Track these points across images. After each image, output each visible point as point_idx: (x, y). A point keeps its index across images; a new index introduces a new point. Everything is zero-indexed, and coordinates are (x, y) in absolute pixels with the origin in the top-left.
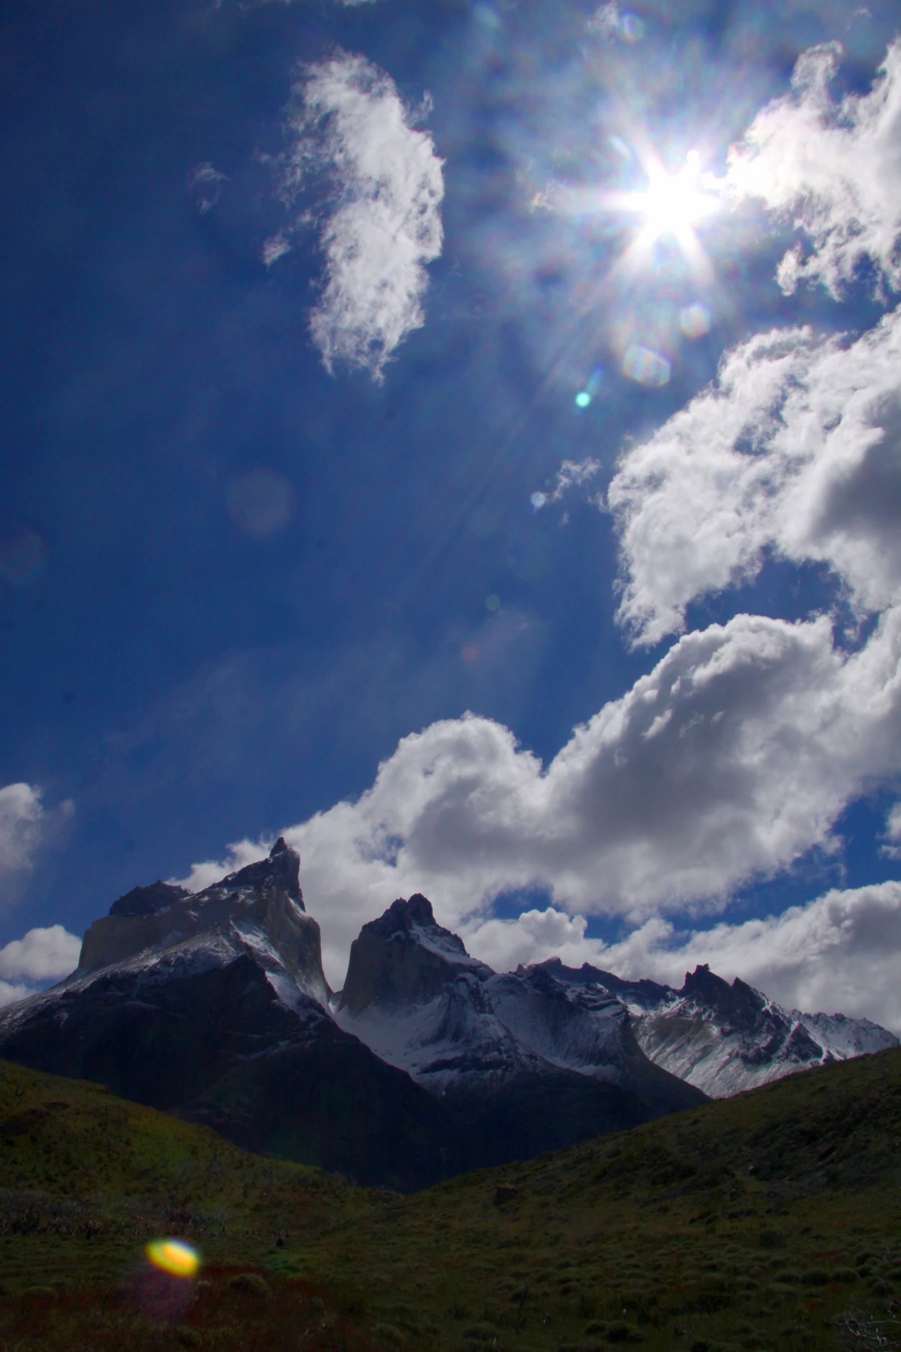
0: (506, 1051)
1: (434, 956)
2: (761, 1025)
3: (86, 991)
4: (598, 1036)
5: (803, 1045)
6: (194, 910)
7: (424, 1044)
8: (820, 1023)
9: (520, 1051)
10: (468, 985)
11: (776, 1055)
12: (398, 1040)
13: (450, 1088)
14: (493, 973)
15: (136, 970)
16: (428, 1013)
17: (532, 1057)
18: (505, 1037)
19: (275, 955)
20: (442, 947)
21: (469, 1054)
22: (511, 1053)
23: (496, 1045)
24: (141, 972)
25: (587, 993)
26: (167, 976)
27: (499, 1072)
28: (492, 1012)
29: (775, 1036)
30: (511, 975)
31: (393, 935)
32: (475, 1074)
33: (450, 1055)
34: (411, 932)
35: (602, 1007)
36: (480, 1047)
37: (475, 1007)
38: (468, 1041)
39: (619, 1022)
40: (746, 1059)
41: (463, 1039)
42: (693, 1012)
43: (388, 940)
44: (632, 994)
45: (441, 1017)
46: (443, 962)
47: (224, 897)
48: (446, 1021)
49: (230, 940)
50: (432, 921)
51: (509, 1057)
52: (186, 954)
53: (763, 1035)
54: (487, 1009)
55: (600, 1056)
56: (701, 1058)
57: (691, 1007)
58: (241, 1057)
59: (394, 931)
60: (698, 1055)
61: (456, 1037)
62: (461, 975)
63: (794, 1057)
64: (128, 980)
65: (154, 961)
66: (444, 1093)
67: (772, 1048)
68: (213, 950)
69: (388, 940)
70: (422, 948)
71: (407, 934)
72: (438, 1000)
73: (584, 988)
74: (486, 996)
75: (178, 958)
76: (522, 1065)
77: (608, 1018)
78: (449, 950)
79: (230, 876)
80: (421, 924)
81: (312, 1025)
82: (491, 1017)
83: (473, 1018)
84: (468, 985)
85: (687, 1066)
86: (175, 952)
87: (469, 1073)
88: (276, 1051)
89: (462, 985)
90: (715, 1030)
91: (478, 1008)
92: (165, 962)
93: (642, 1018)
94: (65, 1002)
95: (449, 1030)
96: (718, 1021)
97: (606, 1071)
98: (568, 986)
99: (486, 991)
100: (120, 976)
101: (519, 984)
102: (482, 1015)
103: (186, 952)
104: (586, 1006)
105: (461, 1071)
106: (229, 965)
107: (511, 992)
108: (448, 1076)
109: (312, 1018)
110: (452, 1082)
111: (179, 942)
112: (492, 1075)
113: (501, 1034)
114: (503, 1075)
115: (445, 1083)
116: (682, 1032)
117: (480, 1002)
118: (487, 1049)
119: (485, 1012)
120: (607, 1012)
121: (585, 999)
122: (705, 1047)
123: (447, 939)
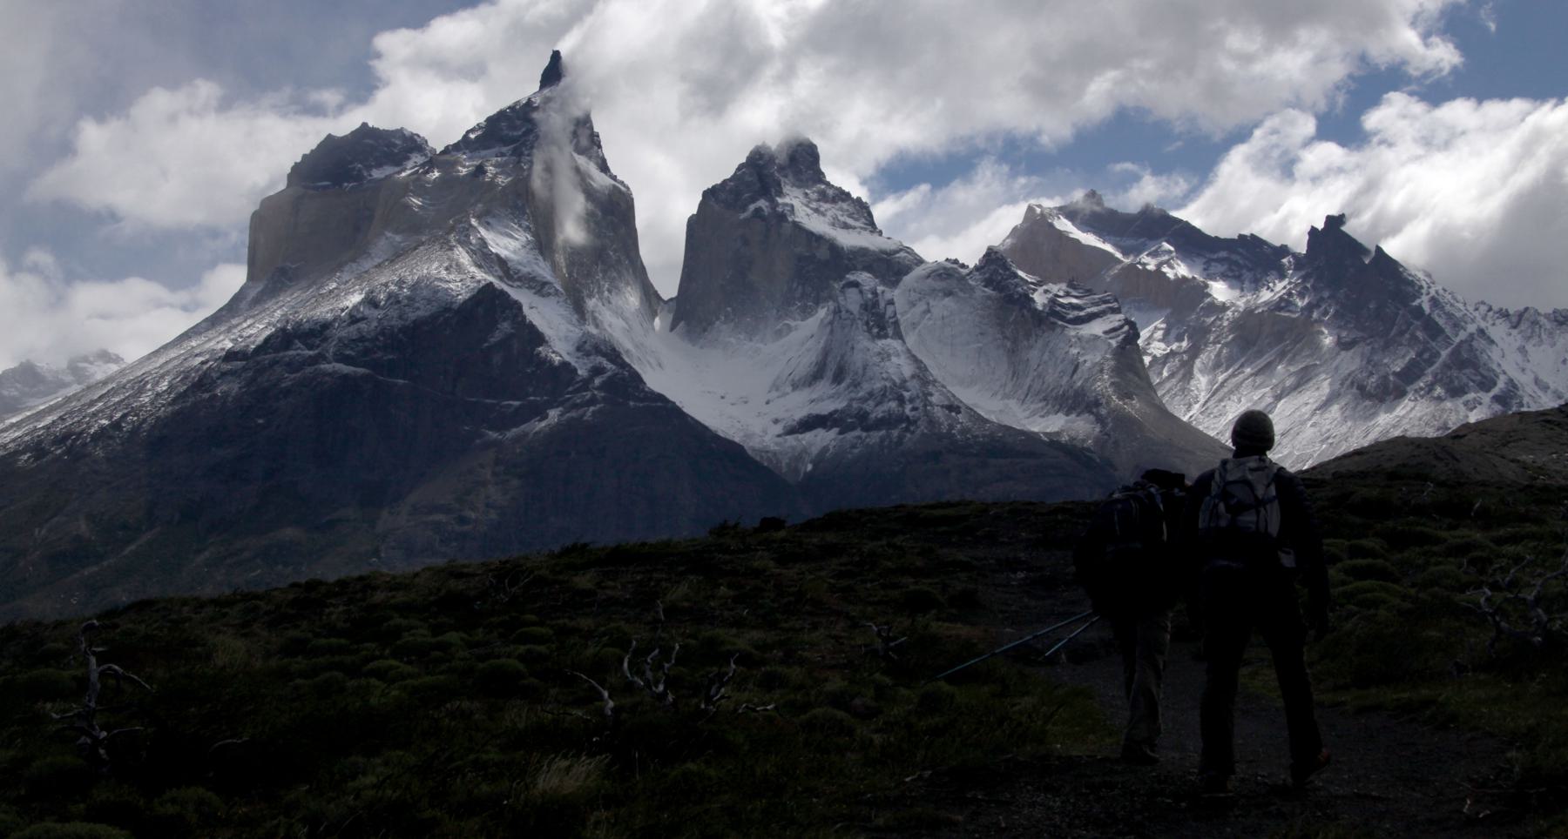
0: (911, 400)
1: (816, 239)
2: (1402, 333)
3: (261, 349)
4: (1075, 371)
5: (1465, 369)
6: (417, 195)
7: (795, 387)
8: (1523, 326)
9: (934, 399)
10: (861, 292)
11: (1415, 386)
12: (741, 391)
13: (819, 460)
14: (920, 261)
15: (329, 316)
16: (803, 336)
17: (953, 408)
18: (913, 377)
19: (543, 270)
20: (835, 223)
21: (855, 405)
22: (918, 403)
23: (896, 391)
24: (335, 320)
25: (1068, 294)
26: (375, 324)
27: (895, 433)
28: (898, 335)
29: (1419, 354)
30: (949, 265)
31: (752, 207)
32: (859, 437)
33: (825, 408)
34: (780, 200)
35: (1091, 317)
36: (871, 394)
37: (869, 330)
38: (856, 385)
39: (1114, 343)
40: (1363, 392)
41: (848, 381)
42: (1300, 303)
43: (742, 216)
44: (1220, 261)
45: (822, 344)
46: (833, 247)
47: (464, 171)
48: (826, 353)
49: (472, 253)
50: (819, 177)
51: (914, 409)
52: (401, 288)
53: (1402, 350)
54: (890, 331)
55: (1075, 401)
56: (1297, 387)
57: (1301, 295)
58: (493, 435)
59: (754, 200)
60: (1288, 383)
61: (838, 378)
62: (851, 277)
63: (1439, 391)
64: (316, 333)
65: (356, 298)
66: (810, 467)
67: (1410, 374)
68: (441, 280)
69: (742, 216)
70: (796, 225)
71: (774, 204)
72: (822, 313)
73: (1064, 286)
74: (889, 312)
75: (390, 296)
76: (932, 422)
77: (1096, 337)
78: (846, 226)
79: (472, 131)
80: (801, 183)
81: (597, 381)
82: (895, 344)
83: (865, 347)
84: (861, 292)
85: (1269, 400)
86: (387, 280)
87: (851, 435)
88: (543, 424)
89: (852, 293)
90: (1328, 340)
91: (875, 330)
92: (371, 302)
93: (1223, 308)
94: (227, 367)
95: (830, 367)
96: (1339, 321)
97: (1075, 427)
98: (1039, 284)
99: (891, 302)
100: (307, 326)
101: (962, 278)
102: (881, 343)
103: (400, 283)
104: (1063, 318)
105: (840, 433)
106: (465, 302)
107: (949, 293)
108: (821, 439)
109: (597, 371)
110: (825, 449)
111: (398, 255)
112: (882, 440)
113: (908, 370)
114: (901, 438)
115: (815, 451)
116: (1279, 337)
117: (880, 322)
118: (883, 396)
119: (886, 337)
120: (1097, 328)
121: (1062, 305)
122: (1306, 368)
123: (845, 206)
